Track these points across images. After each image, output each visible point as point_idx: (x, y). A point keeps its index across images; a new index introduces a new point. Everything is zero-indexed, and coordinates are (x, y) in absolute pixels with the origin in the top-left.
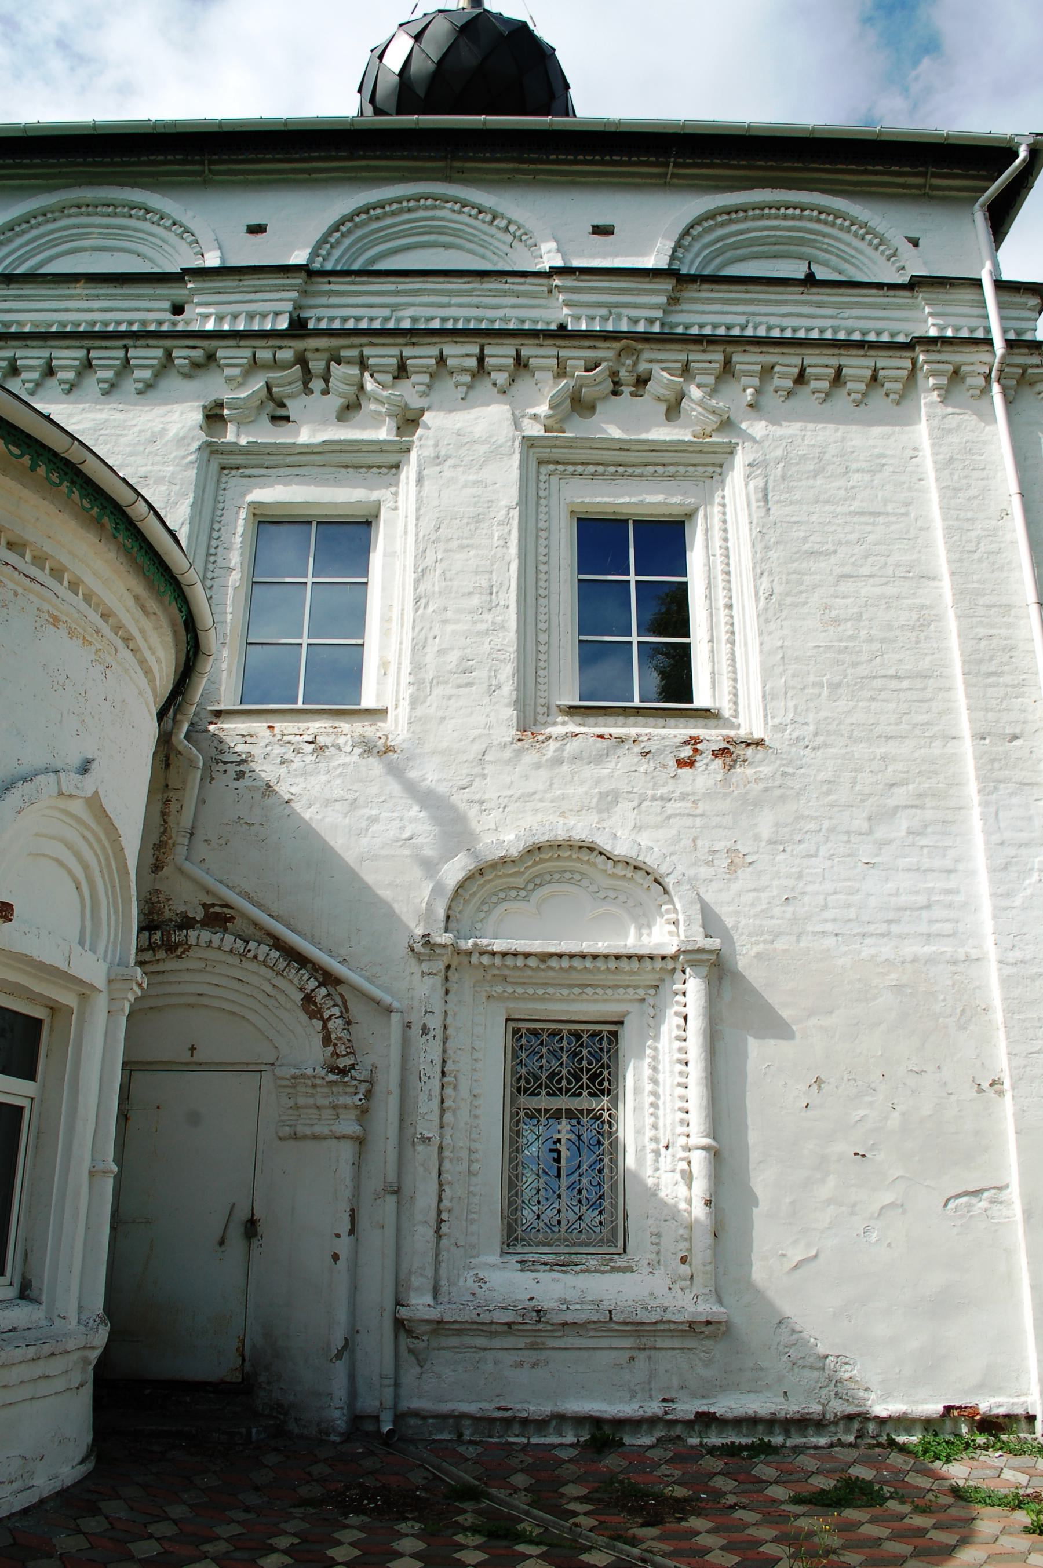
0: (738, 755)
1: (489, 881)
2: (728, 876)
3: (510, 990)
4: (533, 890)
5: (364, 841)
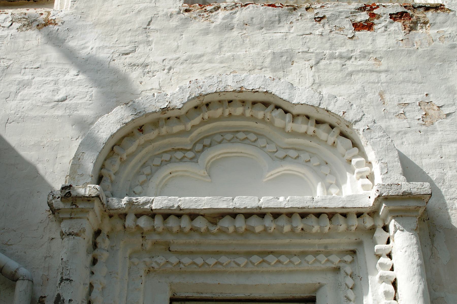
0: (418, 18)
1: (150, 142)
2: (424, 128)
3: (174, 260)
4: (202, 151)
5: (12, 104)
